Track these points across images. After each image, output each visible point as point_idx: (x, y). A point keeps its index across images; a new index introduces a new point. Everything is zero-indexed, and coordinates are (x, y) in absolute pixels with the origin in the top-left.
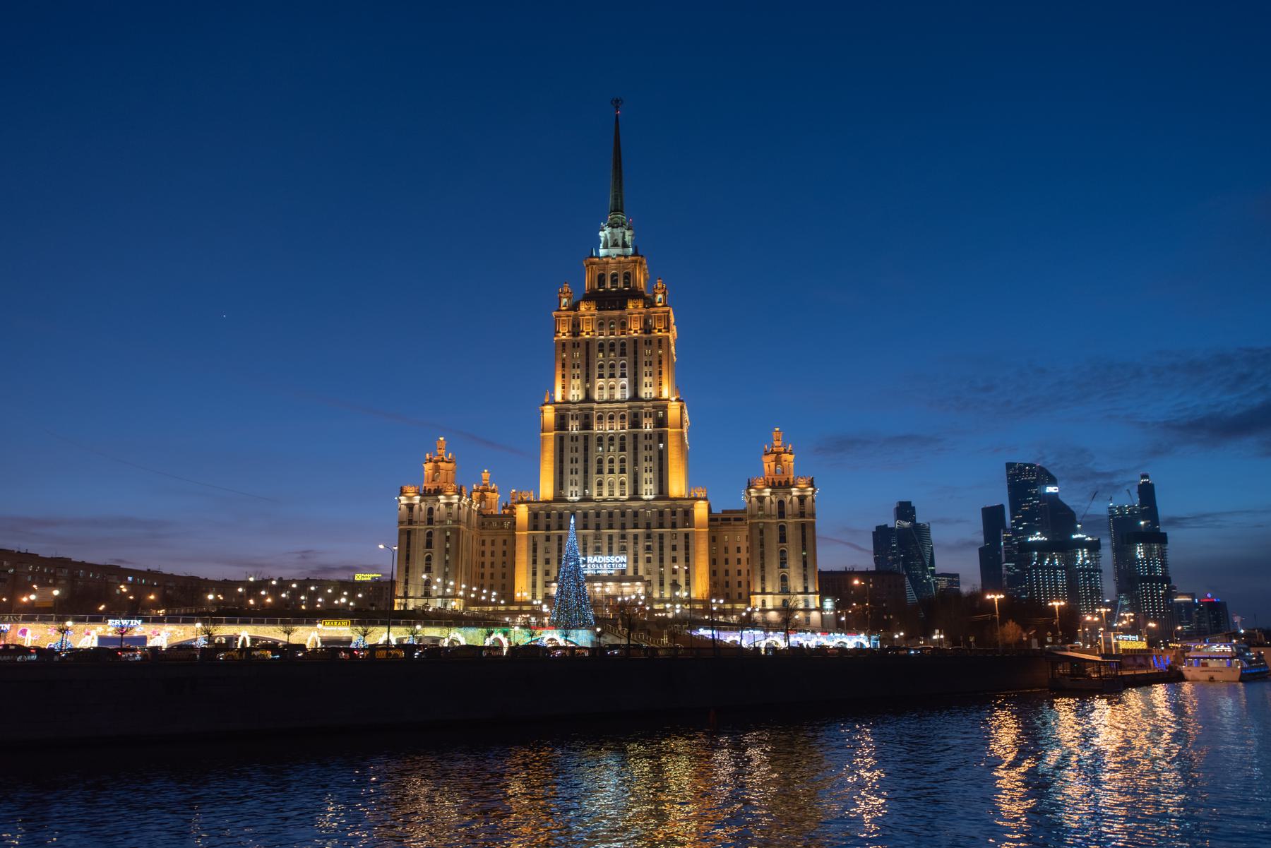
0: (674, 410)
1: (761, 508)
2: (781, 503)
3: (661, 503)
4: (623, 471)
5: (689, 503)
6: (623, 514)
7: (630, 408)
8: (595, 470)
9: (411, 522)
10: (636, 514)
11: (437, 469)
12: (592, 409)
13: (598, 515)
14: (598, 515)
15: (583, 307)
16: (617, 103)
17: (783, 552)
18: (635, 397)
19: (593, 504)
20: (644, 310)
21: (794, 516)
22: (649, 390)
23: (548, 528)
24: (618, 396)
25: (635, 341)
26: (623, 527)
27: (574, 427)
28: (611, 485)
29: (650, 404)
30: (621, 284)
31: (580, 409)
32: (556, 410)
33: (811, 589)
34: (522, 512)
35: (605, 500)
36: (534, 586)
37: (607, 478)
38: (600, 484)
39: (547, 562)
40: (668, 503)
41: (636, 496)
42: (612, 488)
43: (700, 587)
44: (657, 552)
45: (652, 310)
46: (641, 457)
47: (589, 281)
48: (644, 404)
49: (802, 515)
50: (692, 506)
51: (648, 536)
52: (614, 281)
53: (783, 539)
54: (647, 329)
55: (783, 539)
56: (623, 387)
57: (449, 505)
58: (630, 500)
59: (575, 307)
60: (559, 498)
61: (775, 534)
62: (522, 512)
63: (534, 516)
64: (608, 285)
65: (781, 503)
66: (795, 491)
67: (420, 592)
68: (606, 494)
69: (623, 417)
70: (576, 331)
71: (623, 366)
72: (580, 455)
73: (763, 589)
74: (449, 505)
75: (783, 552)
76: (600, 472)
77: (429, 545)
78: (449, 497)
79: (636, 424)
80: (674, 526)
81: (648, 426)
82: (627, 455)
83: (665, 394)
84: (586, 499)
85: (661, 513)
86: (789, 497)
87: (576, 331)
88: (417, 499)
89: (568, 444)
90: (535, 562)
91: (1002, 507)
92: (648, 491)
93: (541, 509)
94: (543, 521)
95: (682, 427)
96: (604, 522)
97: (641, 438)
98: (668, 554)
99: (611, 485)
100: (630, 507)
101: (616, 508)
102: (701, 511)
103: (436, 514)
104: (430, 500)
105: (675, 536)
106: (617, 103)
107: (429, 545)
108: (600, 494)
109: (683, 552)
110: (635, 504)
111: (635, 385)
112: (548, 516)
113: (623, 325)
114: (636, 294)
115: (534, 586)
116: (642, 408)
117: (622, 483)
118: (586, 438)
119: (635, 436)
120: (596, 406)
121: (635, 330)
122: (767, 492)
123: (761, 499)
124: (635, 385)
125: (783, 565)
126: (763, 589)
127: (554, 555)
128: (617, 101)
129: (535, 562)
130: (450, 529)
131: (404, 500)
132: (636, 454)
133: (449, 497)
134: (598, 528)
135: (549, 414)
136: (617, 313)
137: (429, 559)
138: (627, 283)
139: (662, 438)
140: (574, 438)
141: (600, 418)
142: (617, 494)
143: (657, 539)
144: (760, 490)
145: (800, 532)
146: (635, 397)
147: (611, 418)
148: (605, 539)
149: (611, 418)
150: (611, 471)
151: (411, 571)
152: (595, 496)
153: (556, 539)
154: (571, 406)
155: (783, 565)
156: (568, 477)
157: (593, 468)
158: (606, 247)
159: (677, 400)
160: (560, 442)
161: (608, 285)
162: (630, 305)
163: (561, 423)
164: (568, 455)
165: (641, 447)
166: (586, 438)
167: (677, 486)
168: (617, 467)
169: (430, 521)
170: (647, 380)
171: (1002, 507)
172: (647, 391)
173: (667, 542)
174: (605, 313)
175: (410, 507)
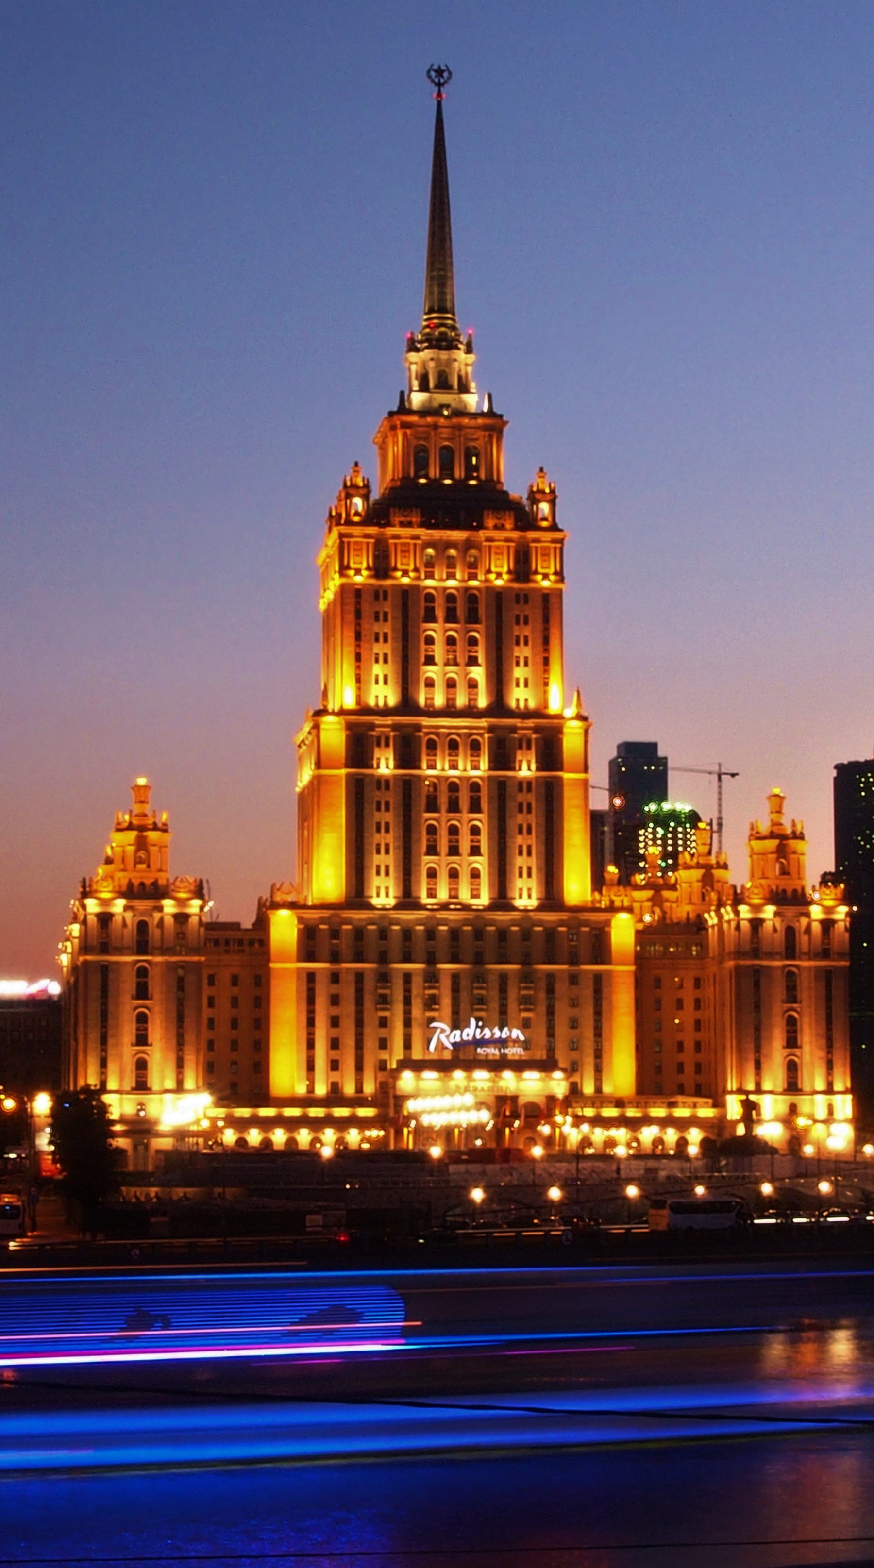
0: (572, 739)
2: (790, 932)
3: (551, 917)
4: (475, 851)
5: (602, 917)
6: (479, 934)
7: (491, 729)
8: (424, 849)
12: (418, 728)
16: (440, 76)
18: (499, 706)
19: (422, 914)
20: (515, 535)
21: (811, 955)
23: (335, 958)
25: (498, 595)
28: (454, 875)
29: (530, 723)
31: (395, 727)
32: (349, 726)
33: (838, 1086)
34: (284, 928)
35: (444, 907)
36: (311, 1067)
37: (441, 862)
38: (432, 874)
40: (563, 916)
41: (502, 900)
42: (459, 886)
44: (542, 1009)
45: (532, 535)
46: (512, 827)
48: (518, 722)
49: (825, 954)
50: (608, 923)
51: (527, 978)
54: (522, 569)
57: (181, 918)
58: (492, 907)
60: (356, 895)
61: (778, 991)
62: (284, 928)
64: (434, 471)
65: (790, 932)
66: (816, 912)
67: (130, 1082)
68: (443, 895)
69: (475, 747)
73: (758, 1084)
77: (142, 992)
78: (182, 903)
79: (502, 759)
80: (574, 961)
81: (526, 769)
83: (554, 707)
84: (408, 901)
85: (550, 933)
86: (804, 921)
87: (382, 568)
90: (311, 1022)
93: (323, 920)
94: (324, 945)
95: (586, 770)
97: (511, 790)
98: (563, 1012)
99: (454, 875)
100: (492, 923)
101: (466, 922)
102: (623, 931)
103: (154, 933)
104: (142, 905)
106: (440, 76)
107: (142, 992)
108: (432, 894)
109: (589, 1010)
110: (502, 917)
111: (499, 681)
115: (311, 1067)
116: (514, 729)
120: (426, 721)
122: (769, 912)
123: (756, 924)
124: (499, 681)
125: (792, 1042)
126: (758, 1084)
127: (348, 1009)
128: (440, 72)
129: (311, 1022)
130: (182, 966)
131: (92, 906)
133: (182, 903)
137: (142, 1019)
140: (383, 783)
141: (432, 746)
143: (543, 984)
144: (756, 908)
146: (499, 706)
147: (453, 746)
149: (453, 746)
150: (454, 851)
151: (110, 1041)
152: (425, 900)
153: (352, 978)
154: (378, 720)
155: (792, 1042)
158: (424, 387)
159: (581, 717)
161: (434, 471)
162: (490, 523)
165: (511, 806)
167: (577, 886)
169: (142, 945)
173: (562, 988)
175: (105, 918)
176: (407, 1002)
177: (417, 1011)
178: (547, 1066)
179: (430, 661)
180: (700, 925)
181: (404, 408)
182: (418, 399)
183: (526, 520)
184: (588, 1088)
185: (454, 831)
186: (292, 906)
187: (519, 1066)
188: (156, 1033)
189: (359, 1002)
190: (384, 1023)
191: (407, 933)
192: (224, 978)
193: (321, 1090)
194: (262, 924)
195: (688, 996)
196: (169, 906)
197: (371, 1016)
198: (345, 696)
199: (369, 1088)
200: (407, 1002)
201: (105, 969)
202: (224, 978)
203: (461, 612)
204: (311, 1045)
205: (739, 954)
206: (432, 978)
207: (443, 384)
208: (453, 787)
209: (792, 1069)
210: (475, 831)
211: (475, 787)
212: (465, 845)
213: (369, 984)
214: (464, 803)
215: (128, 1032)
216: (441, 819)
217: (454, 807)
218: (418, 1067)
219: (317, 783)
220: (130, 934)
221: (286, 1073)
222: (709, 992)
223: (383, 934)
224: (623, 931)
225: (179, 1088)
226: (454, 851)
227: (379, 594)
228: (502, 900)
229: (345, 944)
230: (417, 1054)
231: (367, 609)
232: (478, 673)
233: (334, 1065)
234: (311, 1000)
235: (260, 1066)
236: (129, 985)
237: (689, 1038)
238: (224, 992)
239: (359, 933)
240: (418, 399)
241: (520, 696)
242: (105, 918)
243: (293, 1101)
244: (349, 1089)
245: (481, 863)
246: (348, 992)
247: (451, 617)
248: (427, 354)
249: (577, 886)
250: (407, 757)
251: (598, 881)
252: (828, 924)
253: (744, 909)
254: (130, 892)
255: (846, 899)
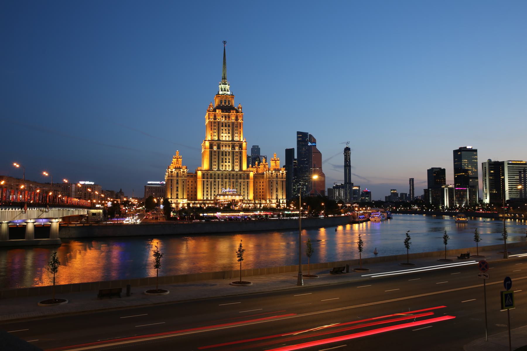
0: (244, 145)
1: (272, 176)
4: (229, 162)
6: (230, 175)
9: (172, 176)
10: (233, 175)
11: (177, 161)
13: (222, 175)
14: (222, 175)
15: (217, 111)
16: (225, 42)
17: (277, 189)
18: (233, 140)
21: (280, 178)
22: (236, 138)
23: (207, 178)
24: (227, 139)
25: (233, 123)
26: (229, 179)
27: (215, 148)
30: (227, 104)
36: (203, 195)
37: (224, 164)
38: (222, 166)
39: (207, 188)
41: (233, 170)
43: (251, 197)
46: (235, 159)
47: (217, 102)
49: (282, 178)
52: (225, 103)
53: (277, 183)
54: (237, 119)
55: (277, 183)
56: (229, 137)
57: (184, 172)
59: (214, 110)
60: (211, 168)
61: (275, 183)
62: (199, 173)
63: (203, 175)
64: (223, 104)
66: (281, 172)
69: (229, 146)
70: (215, 118)
71: (229, 130)
72: (217, 157)
74: (184, 172)
75: (277, 189)
76: (222, 162)
77: (177, 183)
82: (230, 158)
83: (242, 140)
84: (219, 170)
85: (240, 175)
87: (215, 118)
88: (174, 170)
89: (213, 153)
91: (293, 149)
92: (237, 169)
96: (224, 178)
98: (242, 187)
102: (252, 174)
103: (179, 175)
104: (177, 170)
105: (244, 182)
106: (225, 42)
107: (177, 183)
112: (207, 175)
113: (229, 117)
114: (233, 109)
115: (203, 195)
117: (229, 166)
118: (219, 152)
119: (233, 152)
121: (233, 118)
123: (272, 173)
127: (209, 186)
131: (170, 170)
132: (233, 157)
134: (222, 179)
135: (207, 144)
136: (227, 114)
137: (177, 187)
138: (229, 103)
139: (241, 153)
140: (215, 152)
141: (222, 146)
142: (227, 169)
145: (281, 183)
146: (233, 140)
147: (226, 146)
148: (224, 182)
149: (226, 146)
150: (226, 162)
155: (277, 192)
156: (213, 163)
157: (221, 161)
158: (222, 91)
160: (211, 153)
161: (223, 104)
163: (211, 147)
164: (213, 157)
165: (235, 155)
166: (219, 152)
167: (245, 167)
168: (227, 162)
169: (177, 176)
170: (236, 135)
171: (293, 149)
172: (236, 139)
173: (242, 183)
174: (224, 113)
175: (172, 172)
176: (218, 185)
177: (220, 187)
178: (240, 195)
179: (223, 133)
180: (263, 174)
181: (218, 94)
182: (221, 93)
183: (237, 111)
184: (246, 198)
185: (226, 159)
186: (201, 170)
187: (235, 195)
188: (180, 189)
189: (211, 185)
190: (215, 188)
191: (219, 175)
192: (190, 181)
193: (205, 198)
194: (196, 173)
195: (261, 184)
196: (182, 170)
197: (213, 187)
198: (209, 138)
199: (213, 198)
200: (218, 185)
201: (172, 180)
202: (190, 181)
203: (227, 126)
204: (204, 192)
205: (269, 178)
206: (222, 182)
207: (225, 90)
208: (226, 152)
209: (277, 195)
210: (229, 159)
211: (229, 152)
212: (227, 161)
213: (213, 182)
214: (227, 155)
215: (175, 189)
216: (224, 157)
217: (226, 155)
218: (220, 195)
219: (204, 151)
220: (175, 175)
221: (200, 196)
222: (264, 184)
223: (215, 175)
224: (252, 174)
225: (183, 198)
226: (226, 162)
227: (215, 123)
228: (233, 170)
229: (209, 176)
230: (220, 193)
231: (213, 125)
232: (230, 135)
233: (207, 195)
234: (204, 185)
235: (196, 195)
236: (175, 182)
237: (261, 191)
238: (190, 183)
239: (211, 175)
240: (221, 93)
241: (236, 139)
242: (172, 172)
243: (201, 200)
244: (209, 199)
245: (230, 164)
246: (209, 184)
247: (226, 126)
248: (222, 86)
249: (245, 167)
250: (219, 148)
251: (248, 167)
252: (282, 174)
253: (270, 172)
254: (176, 168)
255: (286, 170)
